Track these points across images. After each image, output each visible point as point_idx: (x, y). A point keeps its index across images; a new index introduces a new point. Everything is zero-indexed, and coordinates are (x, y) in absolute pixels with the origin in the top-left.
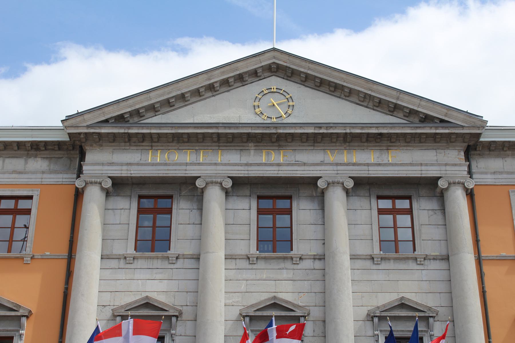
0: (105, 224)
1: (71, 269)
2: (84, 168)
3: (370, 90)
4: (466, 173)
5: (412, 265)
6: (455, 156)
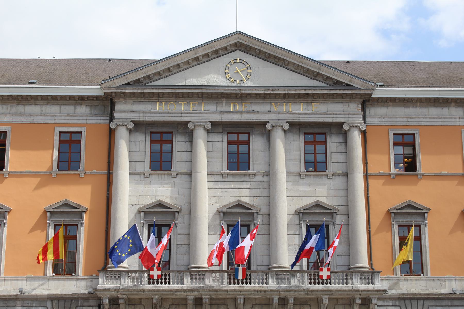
0: (130, 152)
1: (110, 181)
2: (115, 115)
3: (302, 62)
4: (361, 119)
6: (355, 107)
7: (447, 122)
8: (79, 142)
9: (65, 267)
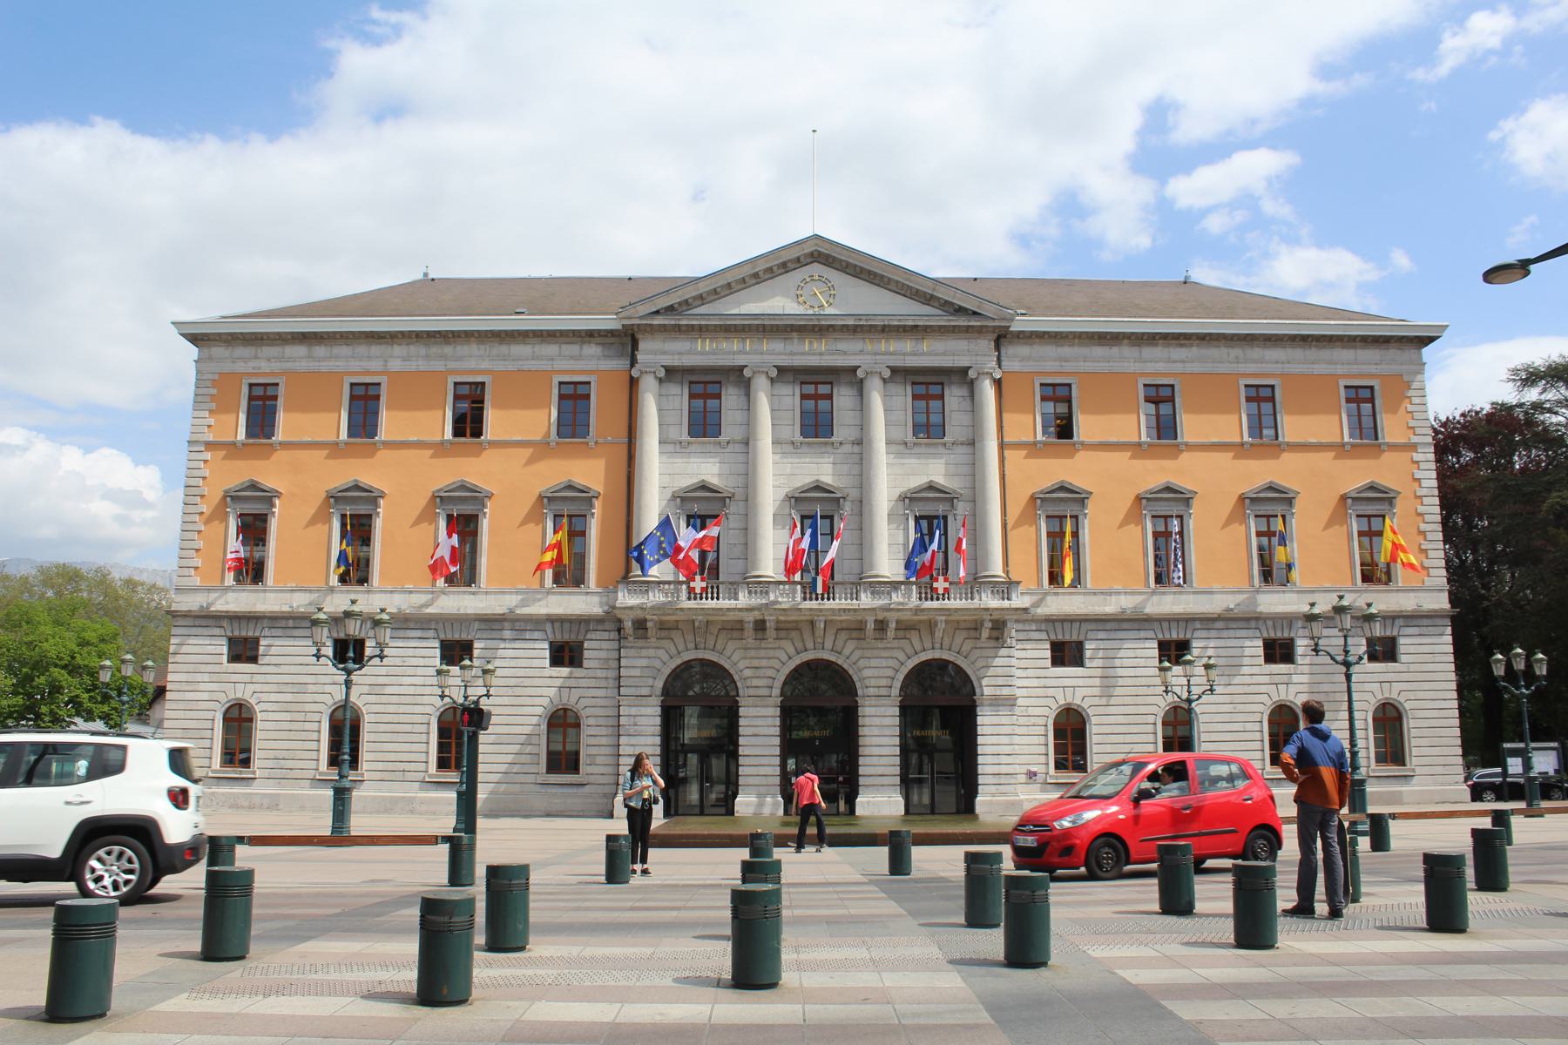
0: (660, 410)
5: (941, 450)
6: (986, 344)
7: (1118, 367)
8: (588, 397)
9: (569, 573)
